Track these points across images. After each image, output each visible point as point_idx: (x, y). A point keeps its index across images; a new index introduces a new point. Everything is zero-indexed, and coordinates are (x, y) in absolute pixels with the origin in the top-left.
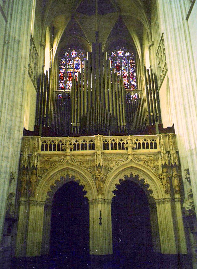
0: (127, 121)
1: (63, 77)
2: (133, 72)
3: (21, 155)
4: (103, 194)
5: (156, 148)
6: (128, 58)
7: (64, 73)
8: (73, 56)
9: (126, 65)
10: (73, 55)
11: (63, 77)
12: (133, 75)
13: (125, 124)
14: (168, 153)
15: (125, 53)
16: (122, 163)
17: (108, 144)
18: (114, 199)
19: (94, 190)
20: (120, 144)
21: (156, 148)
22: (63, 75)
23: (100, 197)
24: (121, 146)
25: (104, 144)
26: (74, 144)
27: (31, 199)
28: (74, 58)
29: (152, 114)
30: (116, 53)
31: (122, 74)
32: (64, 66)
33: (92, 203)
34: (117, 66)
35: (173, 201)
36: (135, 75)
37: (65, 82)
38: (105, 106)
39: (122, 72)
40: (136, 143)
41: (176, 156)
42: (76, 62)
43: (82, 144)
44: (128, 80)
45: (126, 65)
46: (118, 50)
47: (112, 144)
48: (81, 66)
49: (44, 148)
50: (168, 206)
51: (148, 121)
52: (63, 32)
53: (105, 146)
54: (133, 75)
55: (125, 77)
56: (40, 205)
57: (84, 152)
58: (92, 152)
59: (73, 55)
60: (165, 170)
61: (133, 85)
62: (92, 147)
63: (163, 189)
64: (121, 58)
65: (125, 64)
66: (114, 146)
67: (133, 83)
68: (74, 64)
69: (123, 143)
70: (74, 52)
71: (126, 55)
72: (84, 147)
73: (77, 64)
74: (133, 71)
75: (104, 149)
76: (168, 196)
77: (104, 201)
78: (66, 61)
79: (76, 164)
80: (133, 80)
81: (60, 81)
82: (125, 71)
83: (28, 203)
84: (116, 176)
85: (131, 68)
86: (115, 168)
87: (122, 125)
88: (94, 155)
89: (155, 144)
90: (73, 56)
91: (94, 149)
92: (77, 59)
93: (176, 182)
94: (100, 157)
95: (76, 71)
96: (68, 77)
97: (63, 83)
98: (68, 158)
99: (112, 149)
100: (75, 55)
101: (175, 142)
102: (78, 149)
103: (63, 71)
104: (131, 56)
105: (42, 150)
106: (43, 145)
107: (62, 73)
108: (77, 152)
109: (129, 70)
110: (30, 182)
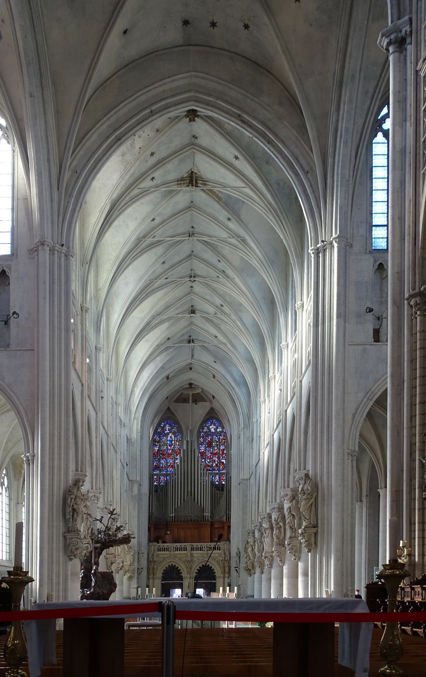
0: (212, 513)
1: (157, 454)
2: (224, 450)
3: (148, 555)
4: (190, 575)
5: (220, 550)
6: (220, 434)
7: (158, 450)
8: (166, 432)
9: (218, 442)
10: (166, 431)
11: (157, 454)
12: (223, 452)
13: (209, 515)
14: (225, 553)
15: (217, 428)
16: (201, 559)
17: (194, 548)
18: (196, 576)
19: (186, 573)
20: (200, 548)
21: (220, 550)
22: (157, 452)
23: (189, 576)
24: (201, 549)
25: (192, 548)
26: (175, 548)
27: (155, 576)
28: (168, 434)
29: (228, 512)
30: (208, 428)
31: (213, 451)
32: (158, 443)
33: (185, 578)
34: (208, 442)
35: (224, 577)
36: (225, 452)
37: (159, 460)
38: (195, 501)
39: (213, 449)
40: (209, 547)
41: (228, 556)
42: (169, 438)
43: (180, 548)
44: (219, 458)
45: (218, 442)
46: (211, 425)
47: (196, 548)
48: (174, 442)
49: (159, 550)
50: (222, 579)
51: (225, 517)
52: (159, 419)
53: (192, 549)
54: (223, 452)
55: (216, 454)
56: (159, 579)
57: (181, 552)
58: (185, 552)
59: (166, 431)
60: (222, 563)
61: (223, 462)
62: (185, 549)
63: (221, 572)
64: (212, 434)
65: (216, 440)
66: (197, 549)
67: (223, 461)
68: (167, 441)
69: (202, 548)
70: (167, 427)
71: (218, 430)
72: (181, 549)
73: (170, 440)
74: (224, 448)
75: (192, 551)
76: (222, 575)
77: (190, 578)
78: (159, 437)
79: (177, 559)
80: (223, 458)
81: (155, 459)
82: (216, 448)
83: (153, 578)
84: (198, 564)
85: (222, 445)
86: (197, 561)
87: (207, 515)
88: (186, 554)
89: (220, 547)
90: (166, 432)
91: (186, 551)
92: (170, 434)
93: (227, 569)
94: (189, 556)
95: (169, 448)
96: (162, 454)
97: (157, 461)
98: (172, 556)
99: (196, 550)
100: (169, 430)
101: (230, 547)
102: (177, 551)
103: (156, 449)
104: (223, 431)
105: (158, 551)
106: (158, 548)
107: (156, 451)
108: (177, 552)
109: (220, 447)
110: (153, 568)
